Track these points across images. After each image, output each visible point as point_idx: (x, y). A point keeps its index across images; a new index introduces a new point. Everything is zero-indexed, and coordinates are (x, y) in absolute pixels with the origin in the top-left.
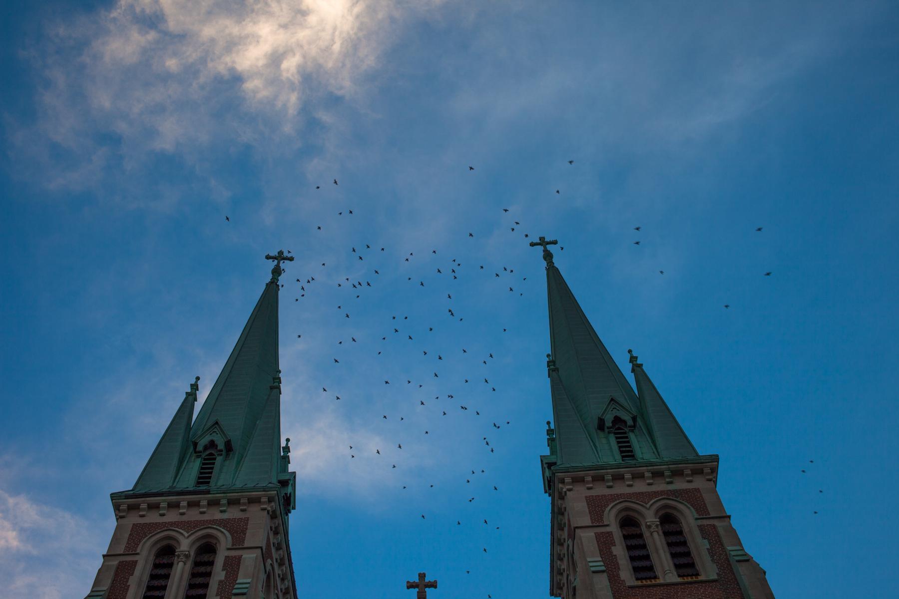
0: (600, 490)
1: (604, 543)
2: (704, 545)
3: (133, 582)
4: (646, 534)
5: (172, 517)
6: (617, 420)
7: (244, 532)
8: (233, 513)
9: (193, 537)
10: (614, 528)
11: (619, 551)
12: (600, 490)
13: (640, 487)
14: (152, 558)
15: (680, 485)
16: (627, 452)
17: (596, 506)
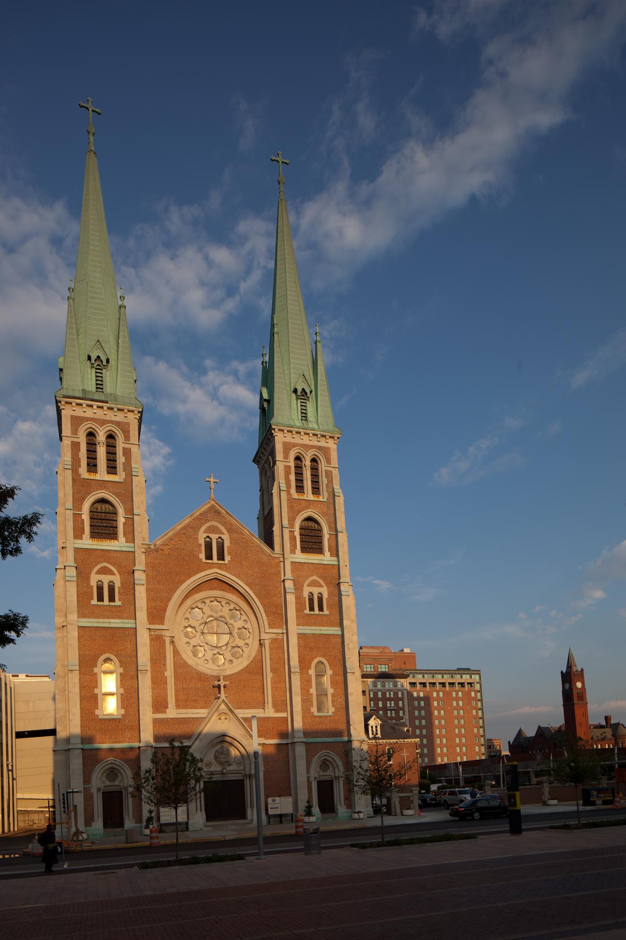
0: (289, 438)
1: (287, 469)
2: (325, 481)
4: (304, 469)
5: (89, 413)
6: (303, 389)
7: (129, 431)
8: (119, 417)
9: (104, 431)
10: (292, 464)
11: (292, 477)
12: (289, 438)
13: (306, 440)
14: (85, 439)
15: (323, 443)
16: (304, 416)
17: (287, 447)
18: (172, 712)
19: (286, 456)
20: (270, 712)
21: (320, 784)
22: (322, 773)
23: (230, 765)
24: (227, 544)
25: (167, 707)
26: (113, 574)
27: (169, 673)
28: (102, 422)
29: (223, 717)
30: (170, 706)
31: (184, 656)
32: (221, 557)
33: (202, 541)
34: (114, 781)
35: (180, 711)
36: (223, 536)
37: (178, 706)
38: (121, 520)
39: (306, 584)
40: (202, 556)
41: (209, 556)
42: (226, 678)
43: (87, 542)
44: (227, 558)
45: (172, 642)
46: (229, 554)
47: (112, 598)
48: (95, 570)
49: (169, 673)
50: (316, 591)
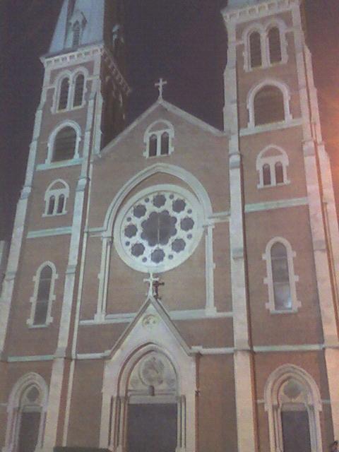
1: (240, 49)
3: (54, 99)
11: (246, 54)
18: (100, 318)
19: (239, 37)
20: (211, 311)
21: (286, 417)
22: (288, 400)
23: (161, 382)
24: (171, 133)
25: (96, 312)
26: (63, 186)
27: (102, 276)
28: (71, 68)
29: (151, 321)
30: (99, 310)
31: (120, 254)
32: (165, 150)
33: (147, 140)
34: (34, 400)
35: (109, 316)
36: (167, 131)
37: (109, 311)
38: (78, 139)
39: (260, 155)
40: (146, 154)
41: (153, 152)
42: (156, 275)
43: (48, 164)
44: (171, 149)
45: (111, 243)
46: (172, 145)
47: (60, 210)
48: (51, 185)
49: (102, 276)
50: (272, 162)
